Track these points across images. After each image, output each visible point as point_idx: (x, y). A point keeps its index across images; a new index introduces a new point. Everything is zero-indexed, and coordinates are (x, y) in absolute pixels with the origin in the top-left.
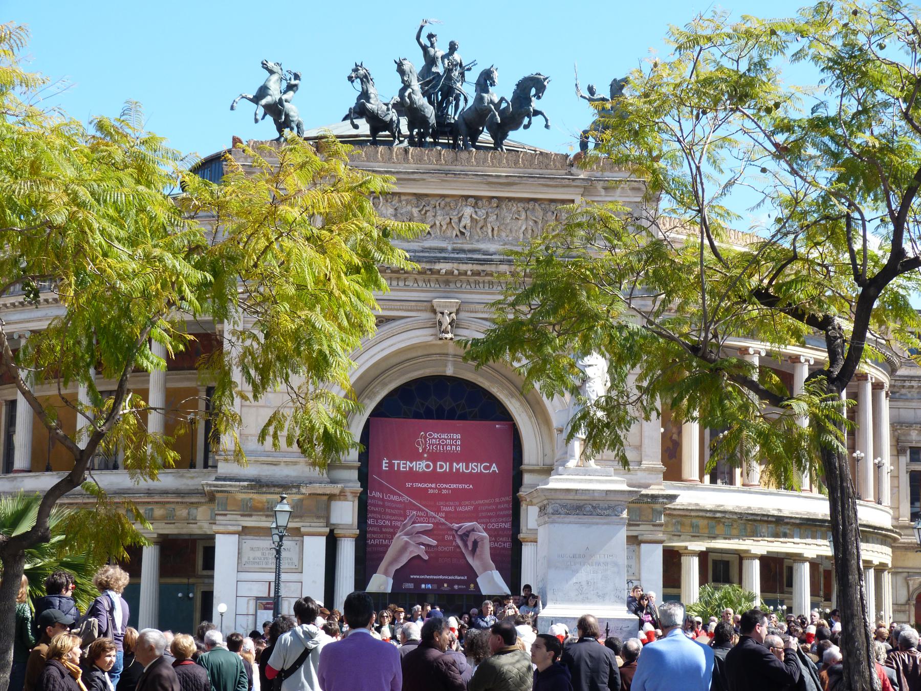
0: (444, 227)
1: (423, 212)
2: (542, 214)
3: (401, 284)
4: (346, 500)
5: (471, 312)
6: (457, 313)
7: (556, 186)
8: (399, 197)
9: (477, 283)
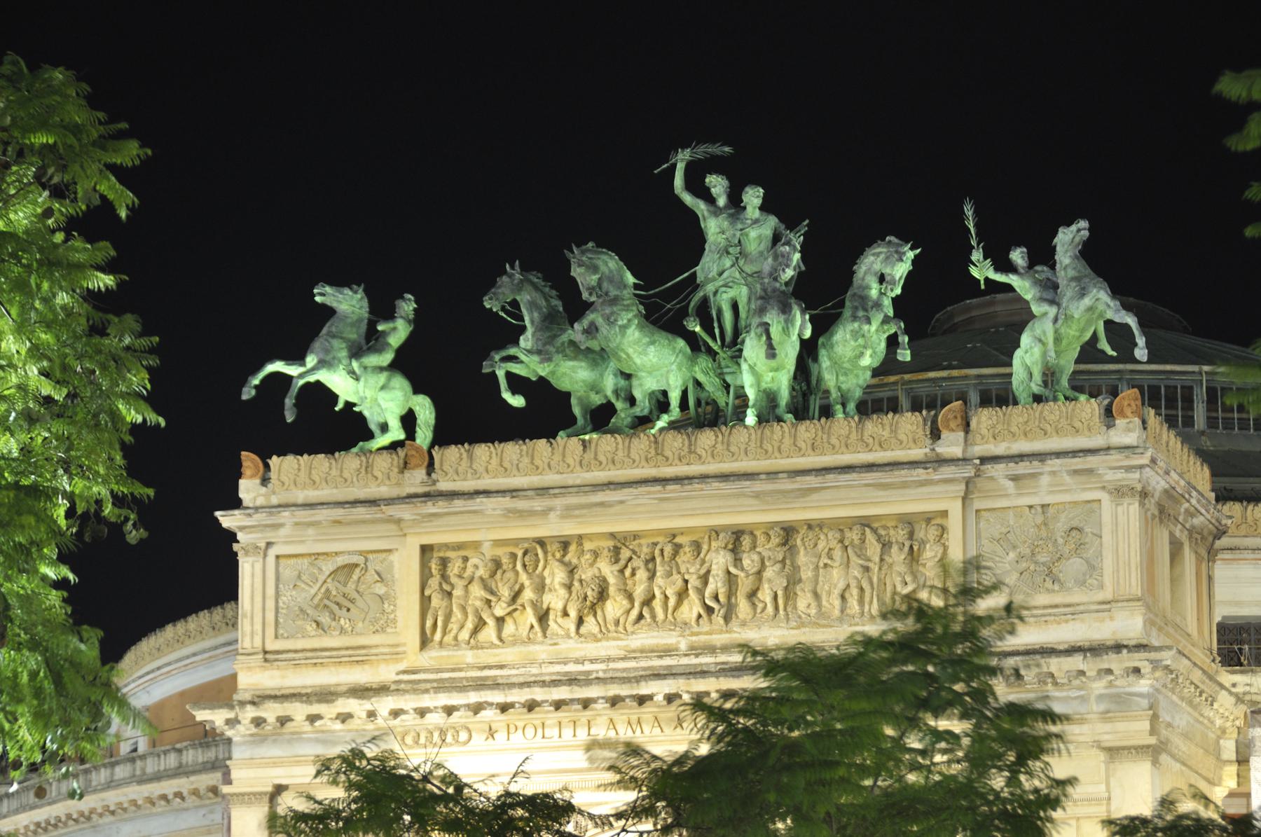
1: (628, 572)
2: (878, 547)
7: (904, 485)
8: (580, 544)
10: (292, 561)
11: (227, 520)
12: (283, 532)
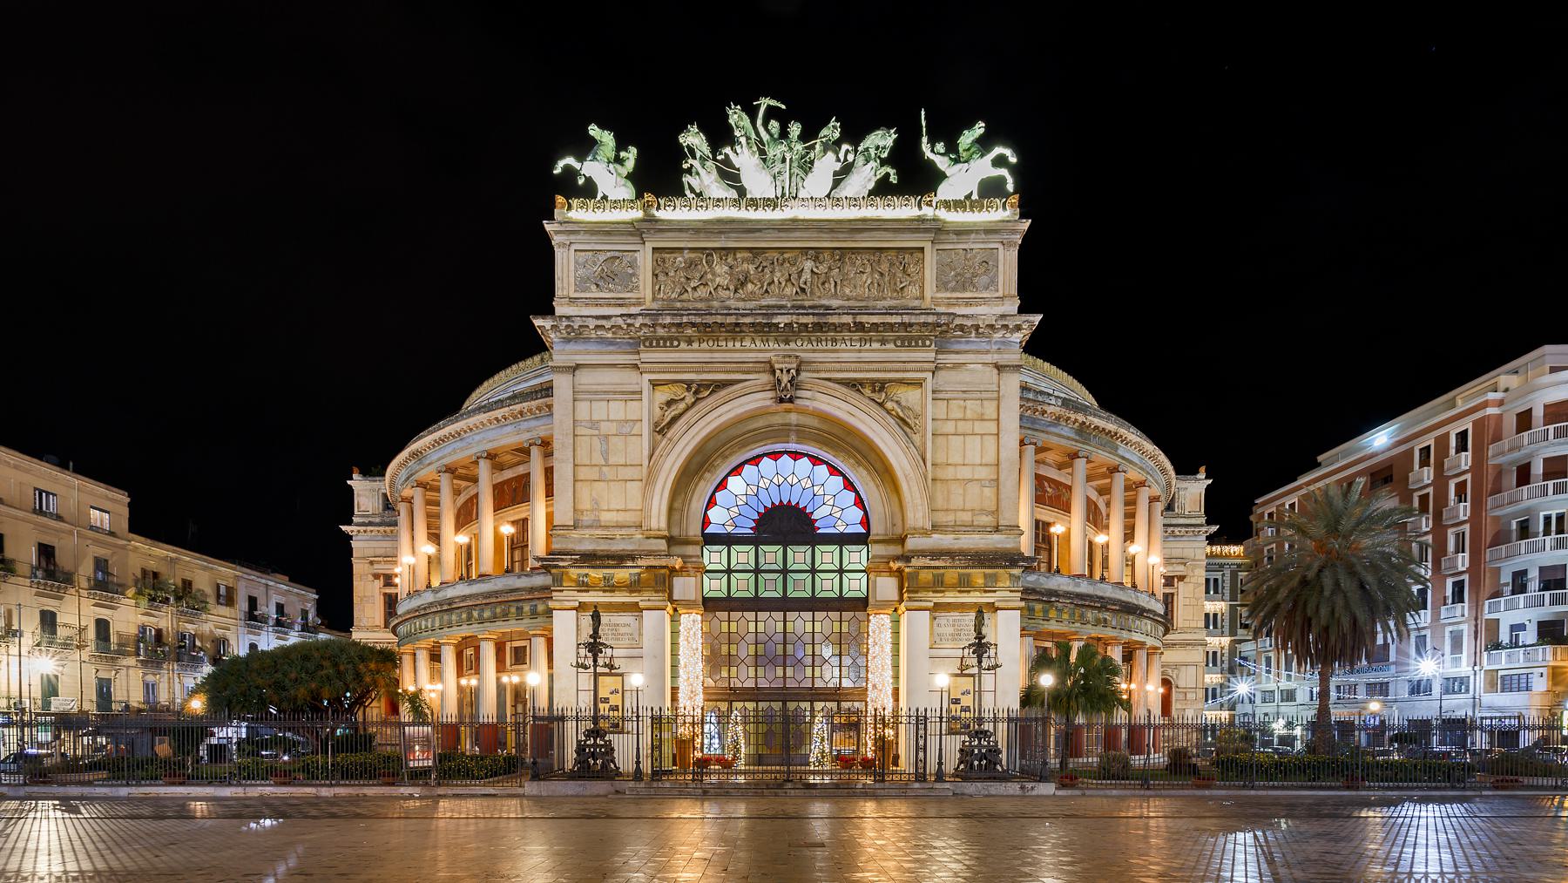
0: (783, 284)
3: (738, 345)
4: (689, 576)
5: (814, 371)
6: (798, 371)
8: (735, 255)
9: (819, 341)
10: (583, 253)
11: (549, 227)
12: (579, 237)
